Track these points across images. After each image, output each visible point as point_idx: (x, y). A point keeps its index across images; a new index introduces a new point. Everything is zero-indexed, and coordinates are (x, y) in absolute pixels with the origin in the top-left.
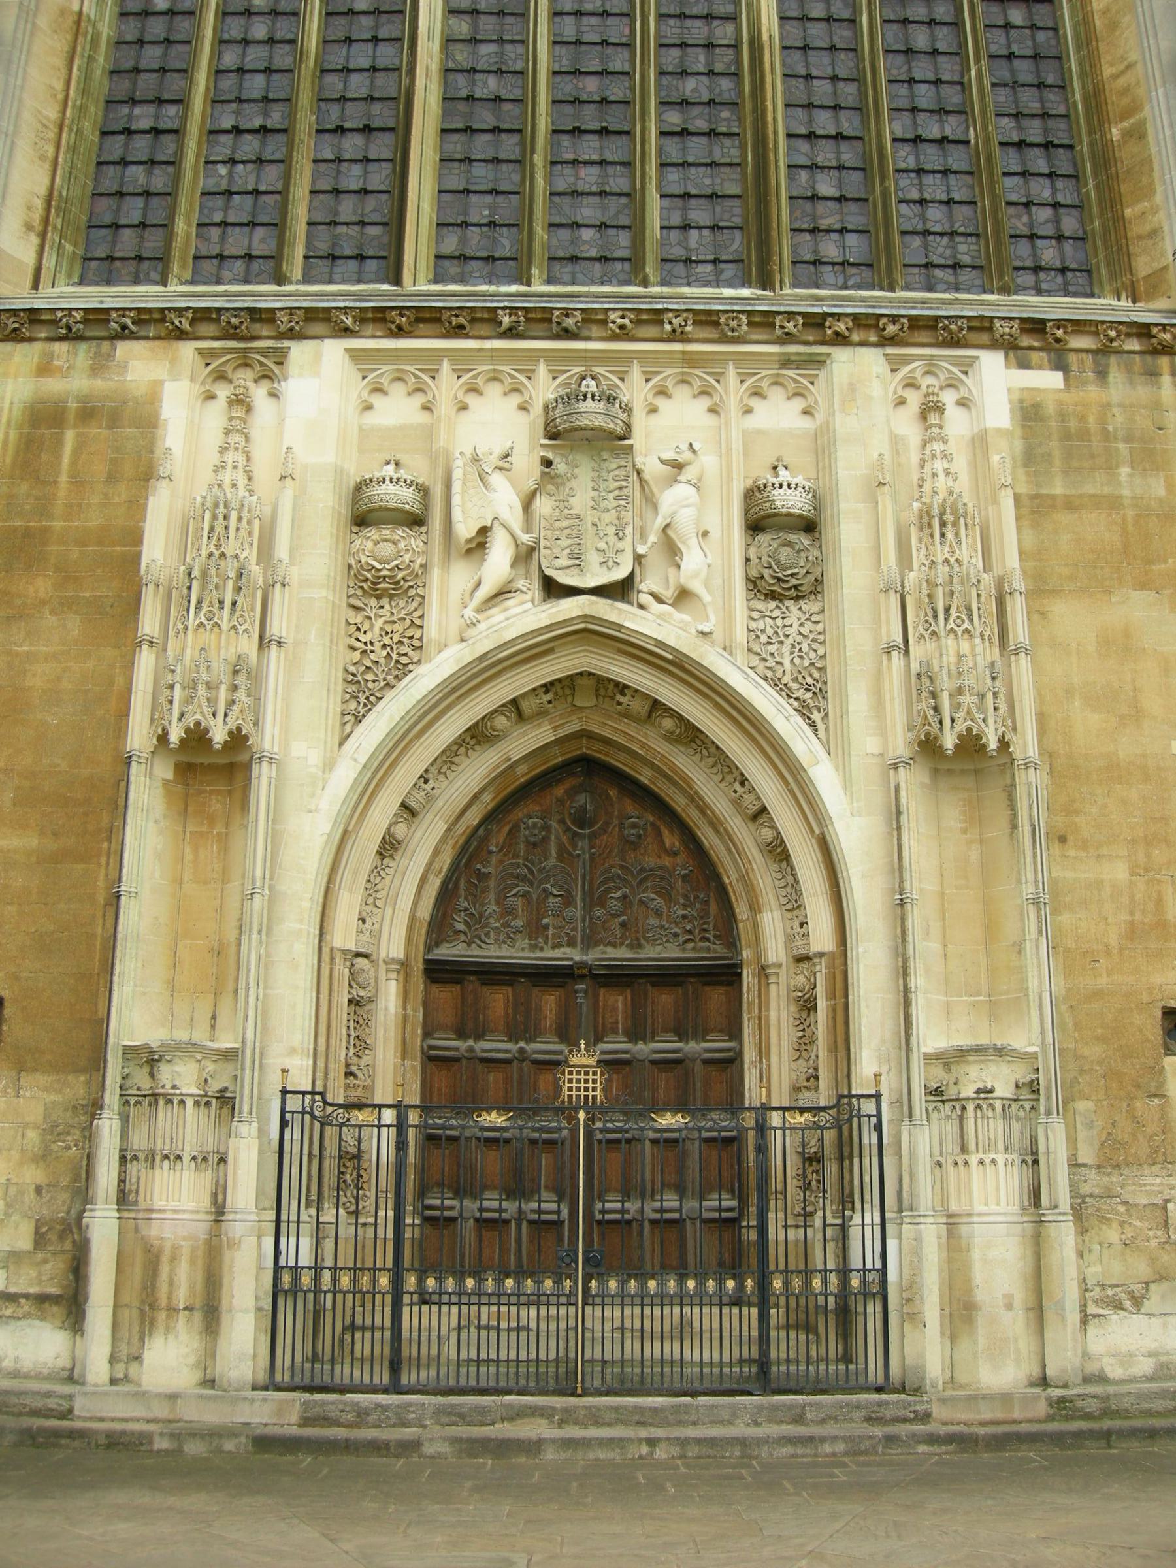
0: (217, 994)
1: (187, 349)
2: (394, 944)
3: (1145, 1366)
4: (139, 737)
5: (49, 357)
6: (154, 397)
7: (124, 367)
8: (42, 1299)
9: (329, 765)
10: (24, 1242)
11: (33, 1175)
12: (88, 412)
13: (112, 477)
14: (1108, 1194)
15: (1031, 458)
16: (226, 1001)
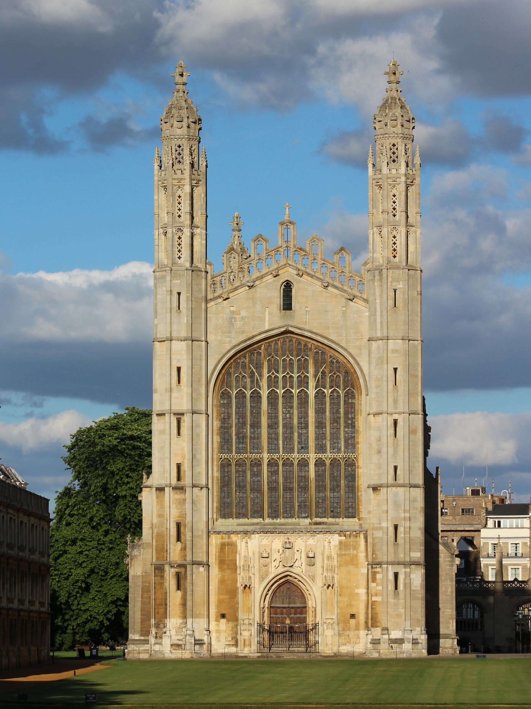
0: (249, 613)
1: (240, 535)
2: (266, 606)
3: (346, 651)
4: (239, 585)
5: (223, 536)
6: (236, 542)
7: (232, 538)
8: (233, 645)
9: (259, 587)
10: (231, 639)
11: (231, 632)
12: (228, 544)
13: (232, 553)
14: (343, 634)
15: (340, 549)
16: (250, 613)
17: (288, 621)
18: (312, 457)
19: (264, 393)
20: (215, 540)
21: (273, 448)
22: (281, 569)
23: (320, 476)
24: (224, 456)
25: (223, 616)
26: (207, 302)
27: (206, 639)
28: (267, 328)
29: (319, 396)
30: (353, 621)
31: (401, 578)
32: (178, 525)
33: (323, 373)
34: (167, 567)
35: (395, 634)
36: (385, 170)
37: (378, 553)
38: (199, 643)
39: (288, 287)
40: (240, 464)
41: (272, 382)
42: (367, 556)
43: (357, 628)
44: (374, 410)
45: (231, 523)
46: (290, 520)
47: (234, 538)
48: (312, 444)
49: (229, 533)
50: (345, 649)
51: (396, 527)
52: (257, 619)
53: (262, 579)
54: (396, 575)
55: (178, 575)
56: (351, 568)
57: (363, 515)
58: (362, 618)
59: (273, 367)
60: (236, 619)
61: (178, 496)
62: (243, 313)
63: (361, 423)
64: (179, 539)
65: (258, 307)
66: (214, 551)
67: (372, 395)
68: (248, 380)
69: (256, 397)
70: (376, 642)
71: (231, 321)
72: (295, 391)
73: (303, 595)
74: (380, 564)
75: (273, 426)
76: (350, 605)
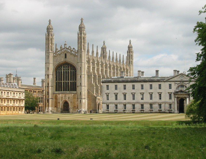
17: (65, 108)
18: (70, 81)
19: (63, 71)
20: (54, 95)
21: (64, 80)
22: (64, 100)
23: (71, 85)
25: (56, 107)
28: (62, 61)
29: (71, 72)
31: (81, 101)
33: (72, 68)
34: (46, 99)
35: (80, 110)
36: (79, 35)
39: (66, 55)
40: (59, 83)
41: (64, 70)
43: (76, 109)
45: (57, 92)
46: (66, 92)
47: (57, 94)
49: (56, 94)
50: (74, 112)
51: (80, 93)
53: (62, 101)
54: (80, 100)
56: (75, 99)
57: (77, 91)
59: (64, 67)
65: (61, 58)
66: (54, 96)
68: (60, 69)
69: (61, 72)
71: (57, 60)
72: (67, 71)
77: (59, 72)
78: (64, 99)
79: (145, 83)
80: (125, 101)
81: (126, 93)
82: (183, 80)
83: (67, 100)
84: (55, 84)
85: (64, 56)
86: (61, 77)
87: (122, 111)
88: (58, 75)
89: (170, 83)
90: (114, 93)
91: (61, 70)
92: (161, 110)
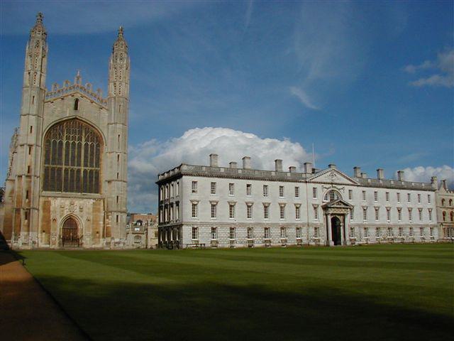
18: (82, 168)
19: (65, 142)
20: (42, 200)
21: (67, 164)
24: (46, 165)
25: (44, 231)
26: (44, 103)
27: (37, 241)
29: (86, 145)
30: (97, 235)
31: (119, 217)
32: (27, 192)
34: (22, 210)
35: (117, 240)
37: (110, 207)
38: (34, 243)
39: (77, 101)
40: (53, 169)
41: (68, 138)
42: (104, 209)
43: (99, 237)
44: (109, 150)
47: (50, 199)
48: (82, 163)
50: (93, 246)
52: (58, 233)
53: (61, 216)
55: (26, 213)
58: (101, 234)
59: (68, 132)
60: (50, 233)
61: (28, 180)
62: (59, 109)
63: (103, 156)
64: (27, 197)
65: (65, 107)
66: (41, 204)
67: (109, 145)
69: (61, 143)
70: (108, 244)
72: (77, 142)
73: (76, 224)
74: (111, 212)
75: (67, 155)
76: (96, 228)
77: (55, 142)
78: (66, 213)
79: (272, 182)
80: (232, 220)
81: (235, 203)
82: (335, 182)
83: (77, 212)
84: (42, 172)
85: (73, 103)
86: (60, 155)
87: (228, 246)
88: (53, 149)
89: (316, 186)
90: (211, 202)
91: (61, 138)
92: (301, 240)
